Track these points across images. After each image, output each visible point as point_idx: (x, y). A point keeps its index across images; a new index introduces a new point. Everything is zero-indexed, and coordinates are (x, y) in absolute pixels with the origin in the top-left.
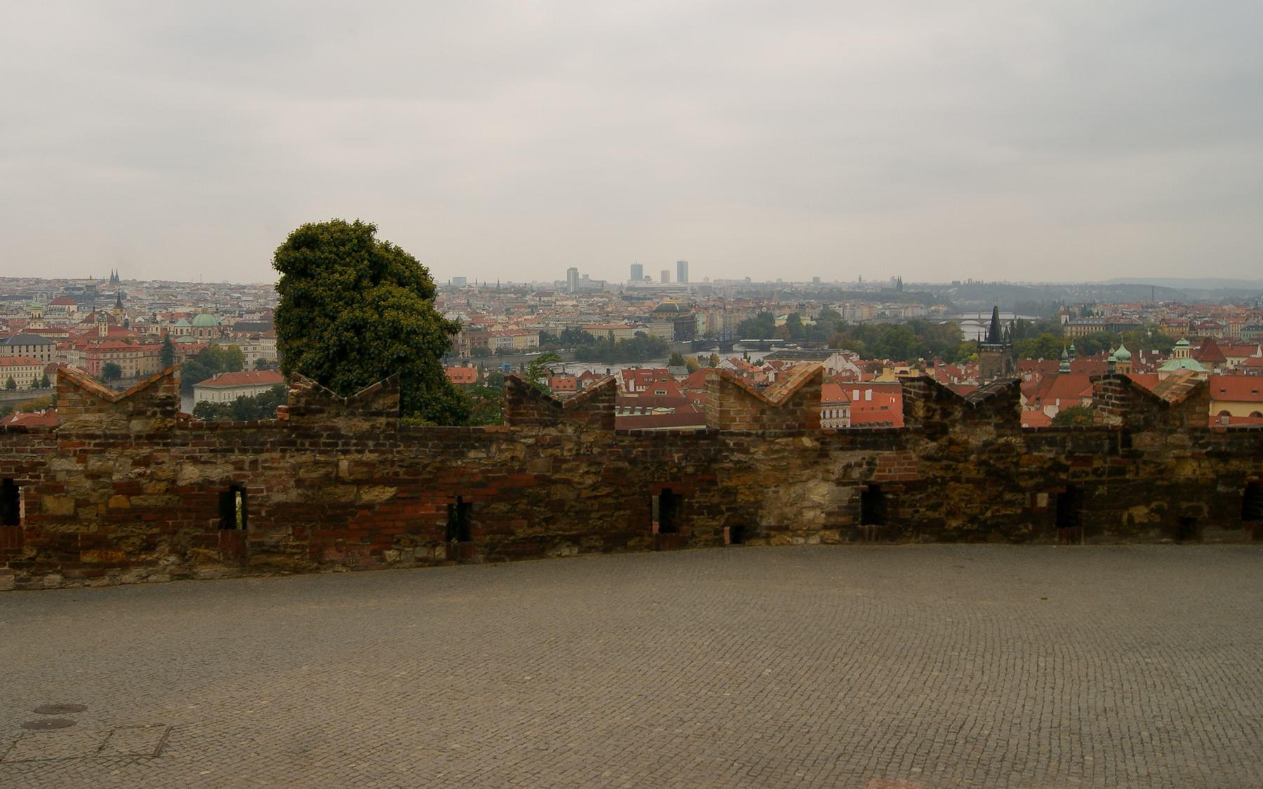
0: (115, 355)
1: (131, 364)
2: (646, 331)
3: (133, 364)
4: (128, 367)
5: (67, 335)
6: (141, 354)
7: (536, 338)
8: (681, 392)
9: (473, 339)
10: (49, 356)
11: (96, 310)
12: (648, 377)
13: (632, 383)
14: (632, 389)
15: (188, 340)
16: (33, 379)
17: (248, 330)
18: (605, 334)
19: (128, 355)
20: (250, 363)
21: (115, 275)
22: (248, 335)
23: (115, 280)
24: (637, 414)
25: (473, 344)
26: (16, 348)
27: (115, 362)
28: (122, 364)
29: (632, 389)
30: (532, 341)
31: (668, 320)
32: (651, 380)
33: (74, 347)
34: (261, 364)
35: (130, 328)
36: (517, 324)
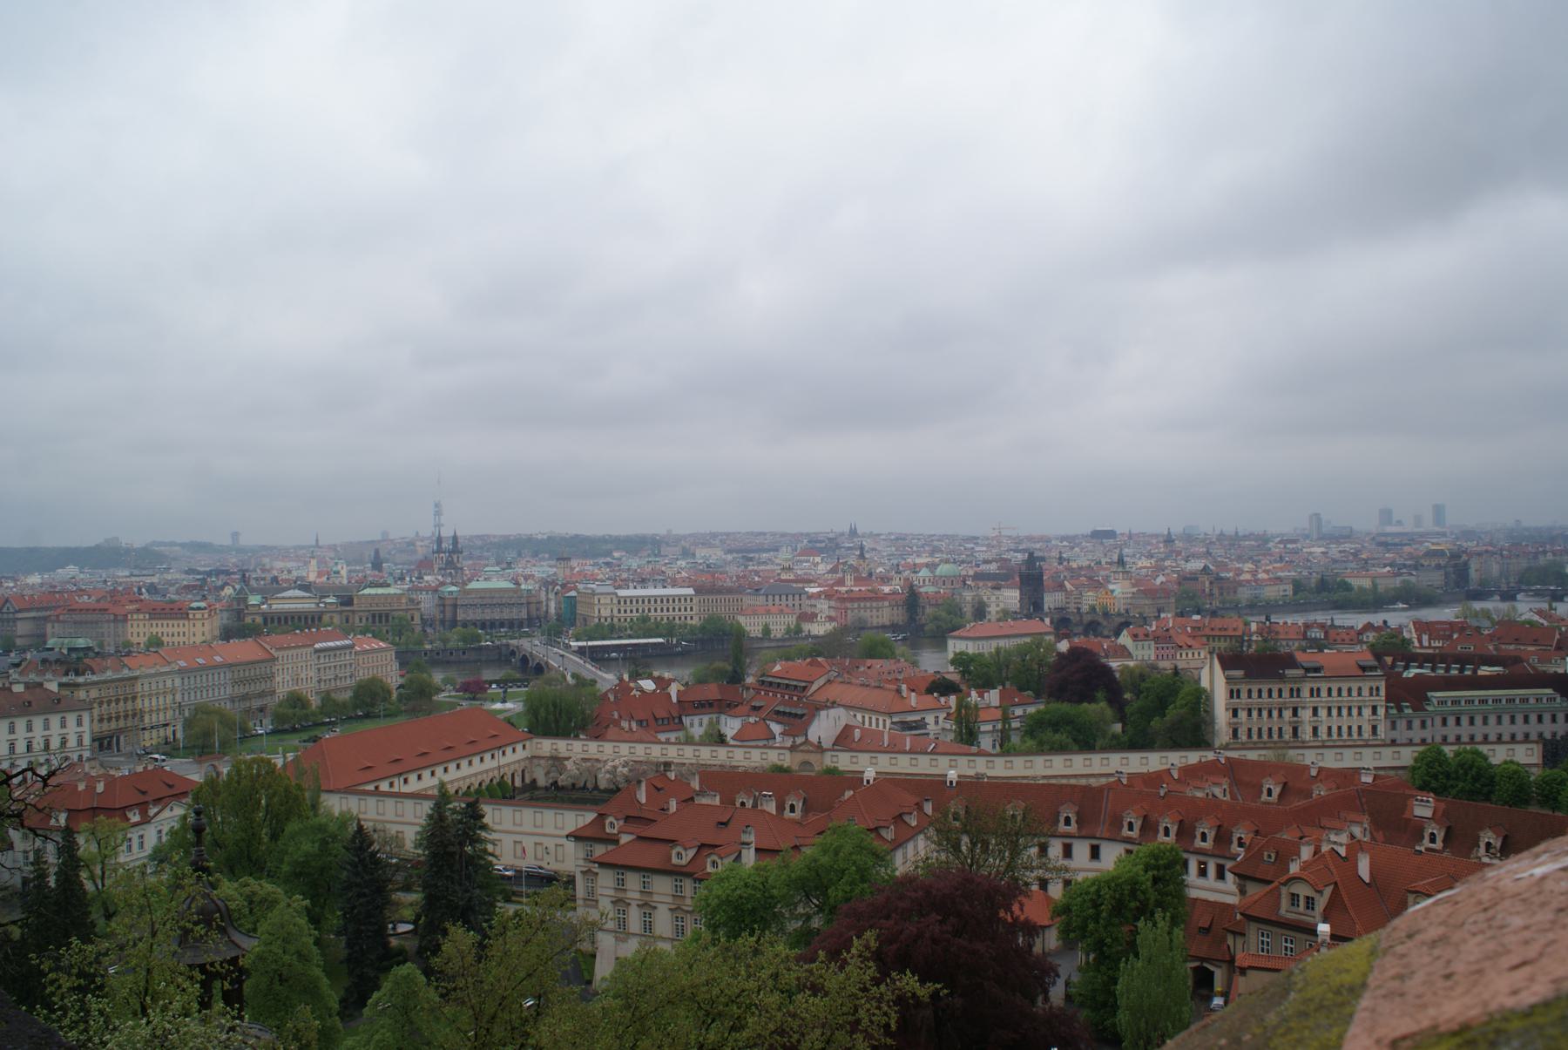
2: (1413, 579)
3: (880, 613)
6: (887, 604)
7: (1289, 589)
8: (1491, 648)
9: (1221, 588)
12: (1445, 630)
13: (1425, 638)
14: (1426, 643)
15: (931, 589)
17: (988, 580)
18: (1366, 583)
19: (874, 604)
20: (994, 613)
22: (990, 584)
24: (1454, 672)
25: (1221, 594)
26: (770, 597)
29: (1426, 643)
30: (1285, 591)
31: (1438, 567)
32: (1448, 633)
33: (823, 597)
34: (1006, 614)
35: (874, 578)
36: (1267, 572)
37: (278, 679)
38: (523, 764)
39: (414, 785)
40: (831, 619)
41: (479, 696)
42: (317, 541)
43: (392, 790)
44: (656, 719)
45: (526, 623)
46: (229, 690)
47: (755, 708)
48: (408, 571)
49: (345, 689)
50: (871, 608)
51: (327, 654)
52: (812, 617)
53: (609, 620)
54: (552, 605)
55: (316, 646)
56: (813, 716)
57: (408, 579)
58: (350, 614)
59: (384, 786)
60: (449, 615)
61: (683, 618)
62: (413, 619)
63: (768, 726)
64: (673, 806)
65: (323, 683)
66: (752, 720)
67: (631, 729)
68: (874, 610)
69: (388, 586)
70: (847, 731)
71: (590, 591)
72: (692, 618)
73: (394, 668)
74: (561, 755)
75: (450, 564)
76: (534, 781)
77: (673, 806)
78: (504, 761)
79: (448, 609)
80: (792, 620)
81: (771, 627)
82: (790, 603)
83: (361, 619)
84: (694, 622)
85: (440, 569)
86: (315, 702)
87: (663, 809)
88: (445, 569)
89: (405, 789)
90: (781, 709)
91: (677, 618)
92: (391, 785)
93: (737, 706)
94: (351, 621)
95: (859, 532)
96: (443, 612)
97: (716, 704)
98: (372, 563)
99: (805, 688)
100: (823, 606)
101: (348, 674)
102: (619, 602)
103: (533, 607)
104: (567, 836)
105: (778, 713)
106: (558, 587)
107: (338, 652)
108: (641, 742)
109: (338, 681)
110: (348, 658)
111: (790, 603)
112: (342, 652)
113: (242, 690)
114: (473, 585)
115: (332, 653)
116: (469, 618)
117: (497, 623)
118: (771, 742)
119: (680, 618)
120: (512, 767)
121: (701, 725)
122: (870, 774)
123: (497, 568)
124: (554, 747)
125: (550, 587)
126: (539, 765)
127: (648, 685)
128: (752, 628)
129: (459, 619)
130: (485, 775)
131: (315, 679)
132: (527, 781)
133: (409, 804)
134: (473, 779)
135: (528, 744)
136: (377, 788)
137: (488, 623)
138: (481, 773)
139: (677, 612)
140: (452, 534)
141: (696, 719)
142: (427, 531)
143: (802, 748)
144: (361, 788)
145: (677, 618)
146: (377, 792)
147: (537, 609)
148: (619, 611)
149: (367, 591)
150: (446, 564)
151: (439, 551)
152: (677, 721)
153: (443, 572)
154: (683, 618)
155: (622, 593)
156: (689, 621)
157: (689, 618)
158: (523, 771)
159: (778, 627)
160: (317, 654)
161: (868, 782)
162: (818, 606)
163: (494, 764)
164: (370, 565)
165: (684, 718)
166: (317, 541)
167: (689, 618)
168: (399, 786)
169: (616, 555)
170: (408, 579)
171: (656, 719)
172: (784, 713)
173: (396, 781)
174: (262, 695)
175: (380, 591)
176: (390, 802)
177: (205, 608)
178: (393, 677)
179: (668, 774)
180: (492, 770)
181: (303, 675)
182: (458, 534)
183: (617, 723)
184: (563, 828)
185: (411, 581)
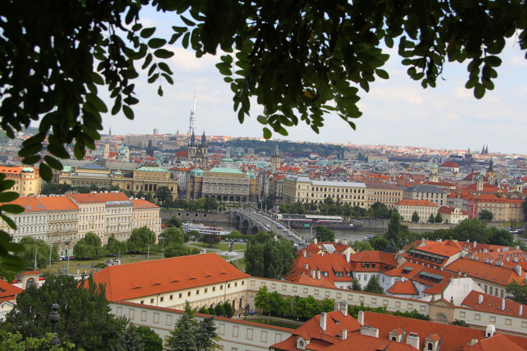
0: (489, 205)
1: (500, 212)
3: (502, 212)
4: (498, 214)
5: (455, 188)
6: (508, 205)
10: (442, 201)
11: (474, 172)
16: (429, 216)
19: (498, 205)
21: (485, 148)
23: (485, 152)
27: (488, 209)
28: (493, 211)
33: (459, 196)
35: (499, 186)
37: (80, 223)
38: (241, 295)
39: (167, 303)
40: (464, 213)
41: (214, 245)
42: (110, 132)
43: (152, 305)
44: (335, 272)
45: (248, 198)
46: (47, 228)
47: (405, 272)
48: (170, 157)
49: (124, 233)
50: (495, 207)
51: (114, 209)
52: (449, 211)
53: (305, 201)
54: (267, 187)
55: (108, 203)
56: (448, 282)
57: (170, 162)
58: (130, 183)
59: (147, 302)
60: (196, 189)
61: (356, 204)
62: (172, 189)
63: (414, 285)
64: (345, 335)
65: (110, 228)
66: (403, 279)
67: (317, 277)
68: (498, 209)
69: (157, 166)
70: (474, 295)
71: (293, 180)
72: (363, 204)
73: (158, 223)
74: (268, 291)
75: (199, 154)
76: (248, 307)
77: (345, 335)
78: (228, 291)
79: (197, 186)
80: (435, 211)
81: (419, 215)
82: (434, 199)
83: (137, 187)
84: (364, 207)
86: (104, 241)
87: (337, 336)
88: (195, 158)
89: (161, 305)
90: (423, 273)
91: (352, 204)
92: (152, 301)
93: (393, 268)
94: (130, 188)
95: (490, 151)
96: (193, 186)
97: (377, 265)
98: (147, 150)
99: (443, 260)
100: (459, 202)
101: (127, 223)
102: (313, 189)
103: (253, 188)
104: (270, 348)
105: (422, 276)
106: (271, 176)
107: (121, 208)
108: (322, 286)
109: (120, 228)
110: (128, 212)
111: (434, 199)
112: (125, 208)
113: (54, 229)
115: (117, 209)
116: (210, 192)
117: (229, 197)
118: (415, 297)
119: (354, 203)
120: (234, 296)
121: (365, 279)
122: (491, 329)
123: (231, 160)
124: (263, 285)
125: (266, 175)
127: (330, 247)
128: (405, 215)
129: (203, 192)
130: (215, 300)
131: (105, 225)
132: (243, 306)
133: (163, 315)
135: (246, 281)
136: (142, 302)
137: (222, 197)
138: (213, 298)
139: (353, 199)
140: (202, 134)
141: (362, 275)
142: (184, 132)
143: (438, 303)
145: (352, 204)
147: (256, 190)
148: (313, 195)
150: (197, 154)
152: (349, 275)
153: (194, 159)
154: (356, 204)
155: (316, 182)
156: (361, 206)
157: (361, 204)
158: (241, 300)
159: (425, 216)
160: (108, 209)
161: (489, 335)
163: (222, 293)
164: (145, 151)
165: (354, 273)
166: (110, 132)
167: (361, 204)
168: (157, 302)
169: (312, 156)
170: (170, 162)
171: (335, 272)
172: (427, 277)
173: (155, 298)
174: (68, 233)
175: (152, 169)
176: (150, 313)
177: (32, 172)
178: (157, 229)
179: (343, 311)
180: (220, 296)
181: (97, 222)
182: (205, 135)
183: (308, 272)
184: (266, 342)
185: (172, 164)
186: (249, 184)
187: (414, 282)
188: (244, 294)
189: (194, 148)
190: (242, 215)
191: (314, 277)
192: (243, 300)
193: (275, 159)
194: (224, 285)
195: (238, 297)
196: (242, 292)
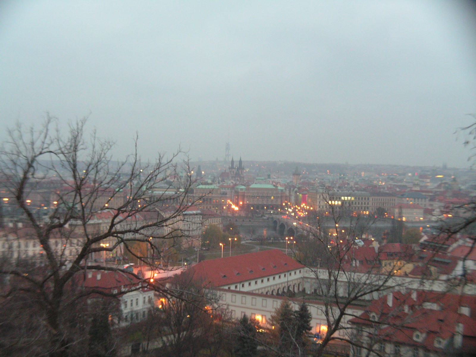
38: (299, 281)
39: (247, 288)
44: (367, 261)
59: (233, 287)
66: (420, 264)
75: (237, 175)
76: (304, 290)
85: (232, 177)
88: (235, 177)
89: (243, 290)
92: (236, 287)
106: (296, 189)
110: (198, 220)
114: (253, 186)
125: (292, 189)
126: (308, 282)
130: (281, 285)
132: (301, 290)
133: (249, 298)
134: (269, 288)
135: (302, 270)
136: (229, 288)
144: (222, 288)
146: (229, 290)
149: (201, 186)
151: (232, 167)
158: (299, 285)
162: (434, 205)
168: (240, 288)
171: (367, 261)
173: (238, 285)
175: (207, 187)
180: (284, 283)
182: (242, 160)
186: (280, 196)
187: (429, 266)
188: (301, 280)
189: (233, 170)
190: (278, 219)
191: (354, 265)
192: (300, 285)
193: (296, 176)
194: (287, 274)
195: (297, 282)
196: (299, 278)
